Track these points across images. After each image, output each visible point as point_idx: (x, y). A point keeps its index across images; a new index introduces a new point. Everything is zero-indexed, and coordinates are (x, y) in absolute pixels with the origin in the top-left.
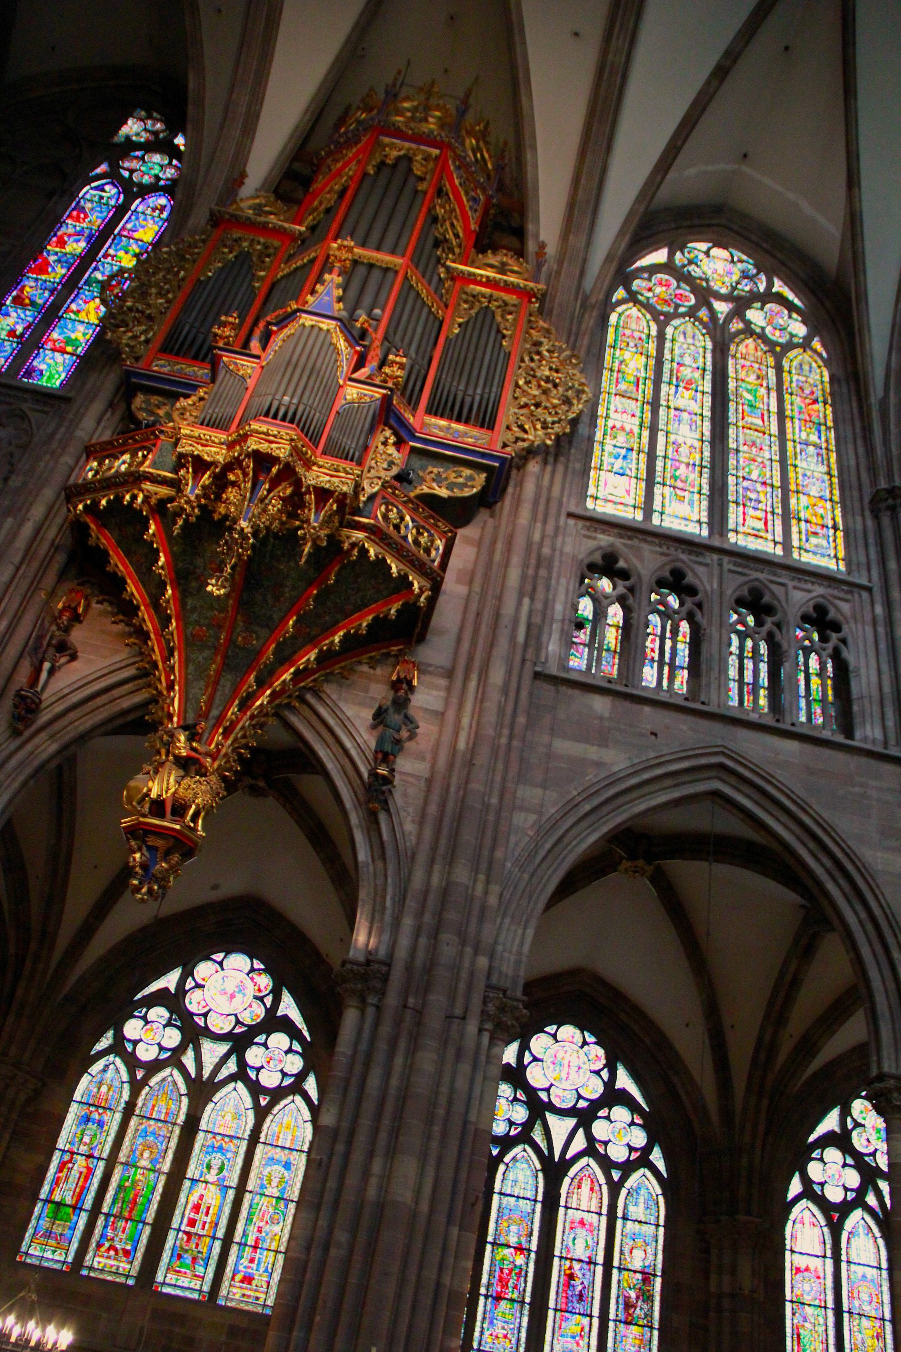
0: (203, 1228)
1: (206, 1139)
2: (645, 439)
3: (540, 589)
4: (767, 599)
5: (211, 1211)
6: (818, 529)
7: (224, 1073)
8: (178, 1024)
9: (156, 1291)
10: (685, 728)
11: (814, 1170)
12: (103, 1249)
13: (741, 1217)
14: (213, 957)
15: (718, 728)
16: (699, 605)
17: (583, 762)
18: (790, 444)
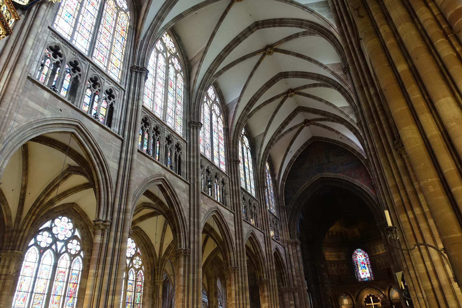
2: (76, 14)
3: (36, 48)
4: (98, 81)
6: (116, 67)
10: (70, 111)
11: (39, 238)
13: (16, 251)
15: (79, 114)
16: (80, 75)
17: (37, 111)
18: (115, 39)
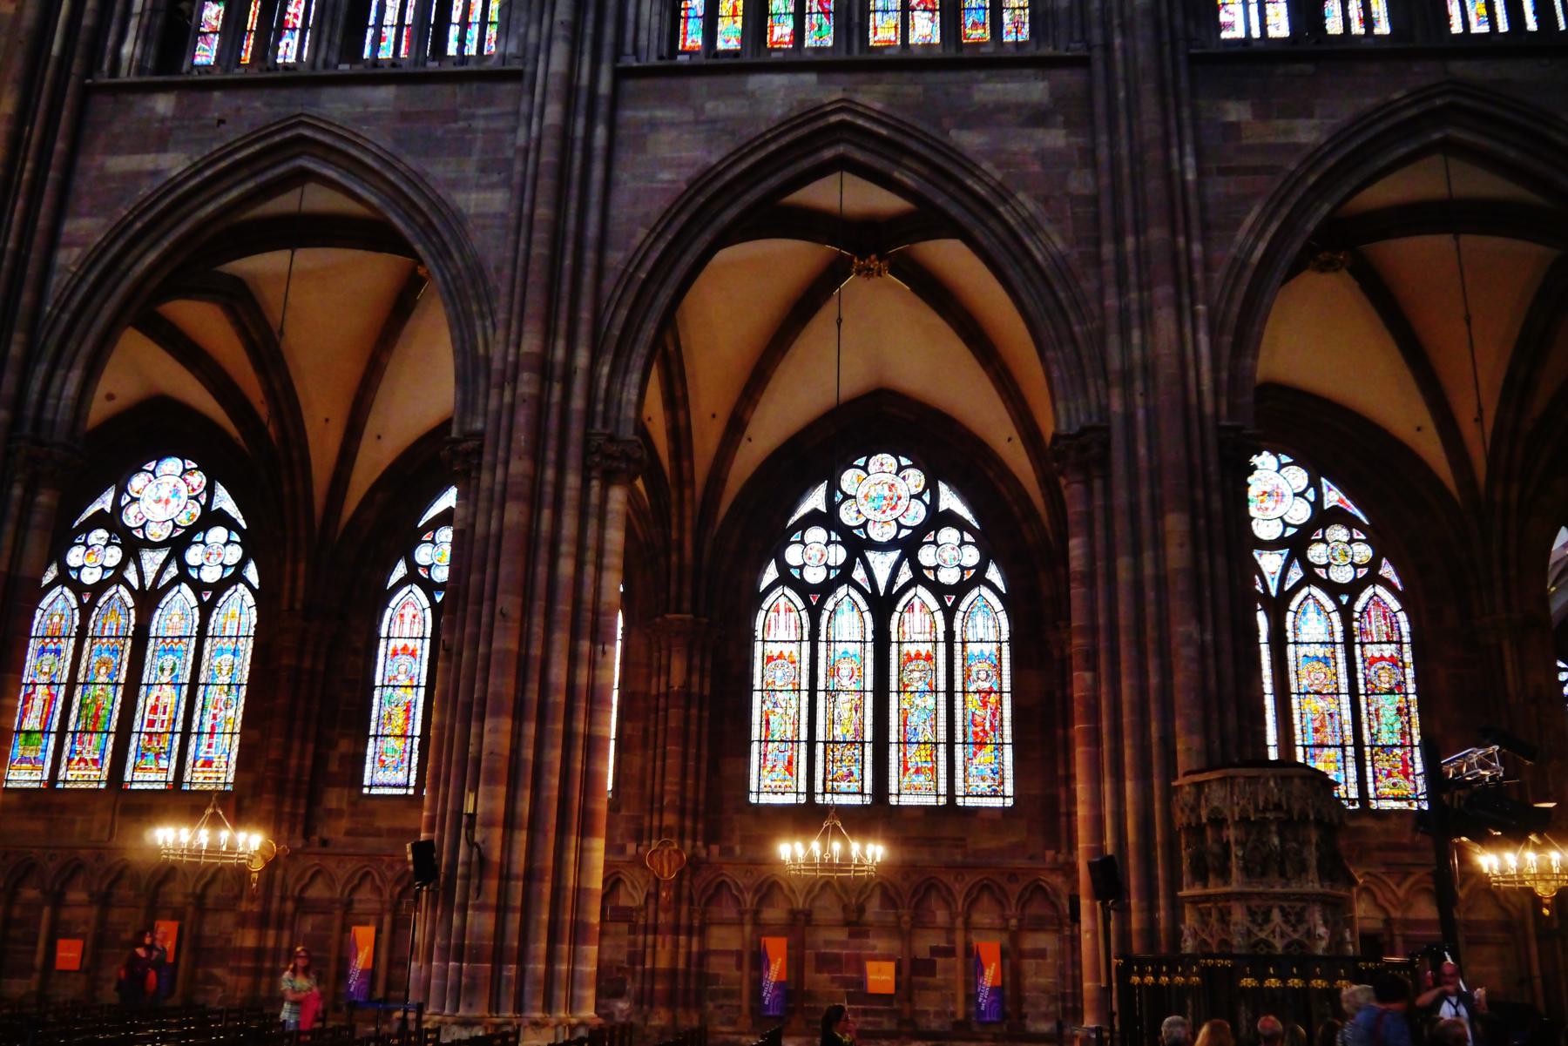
0: (162, 726)
1: (156, 644)
5: (168, 709)
7: (167, 578)
8: (118, 541)
9: (126, 790)
11: (793, 555)
12: (74, 763)
14: (145, 468)
15: (300, 95)
